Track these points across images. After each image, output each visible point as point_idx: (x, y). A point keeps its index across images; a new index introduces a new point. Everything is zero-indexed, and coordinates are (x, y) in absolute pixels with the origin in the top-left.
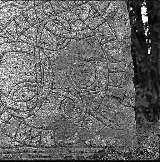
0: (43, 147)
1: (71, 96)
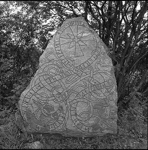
0: (89, 133)
1: (99, 117)
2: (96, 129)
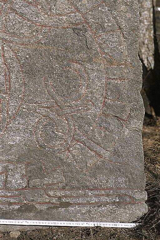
2: (41, 172)
